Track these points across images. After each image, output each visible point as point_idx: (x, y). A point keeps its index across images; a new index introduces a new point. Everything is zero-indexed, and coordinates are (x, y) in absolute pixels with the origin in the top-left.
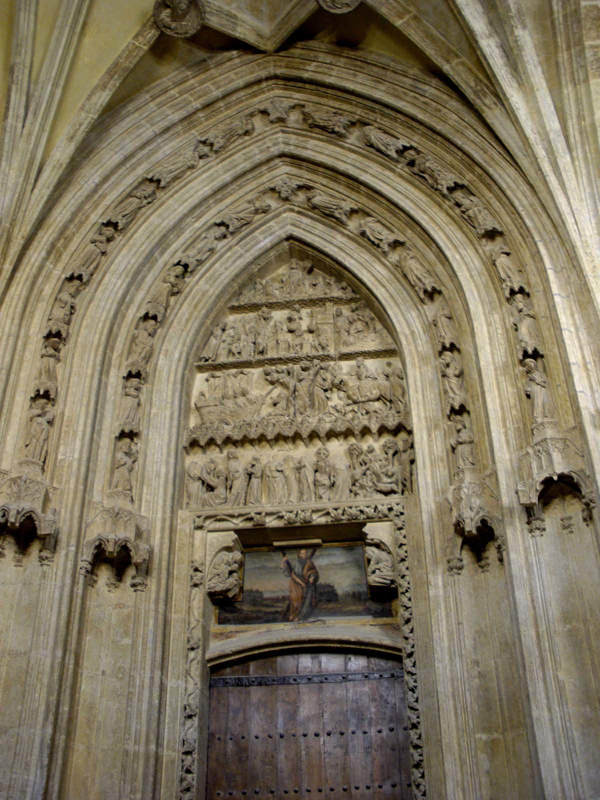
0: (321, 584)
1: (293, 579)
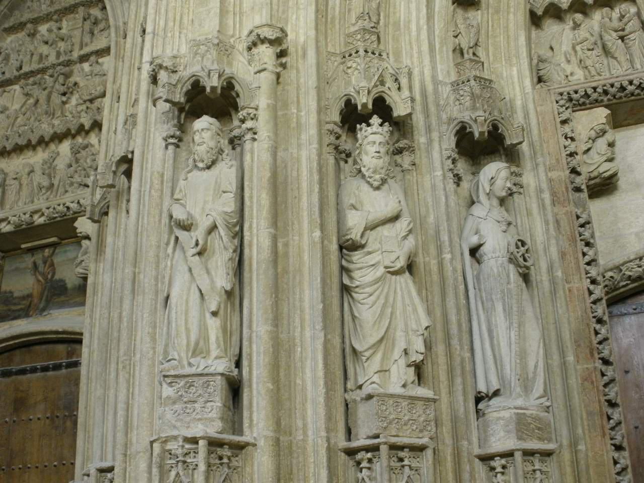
0: (56, 280)
1: (36, 277)
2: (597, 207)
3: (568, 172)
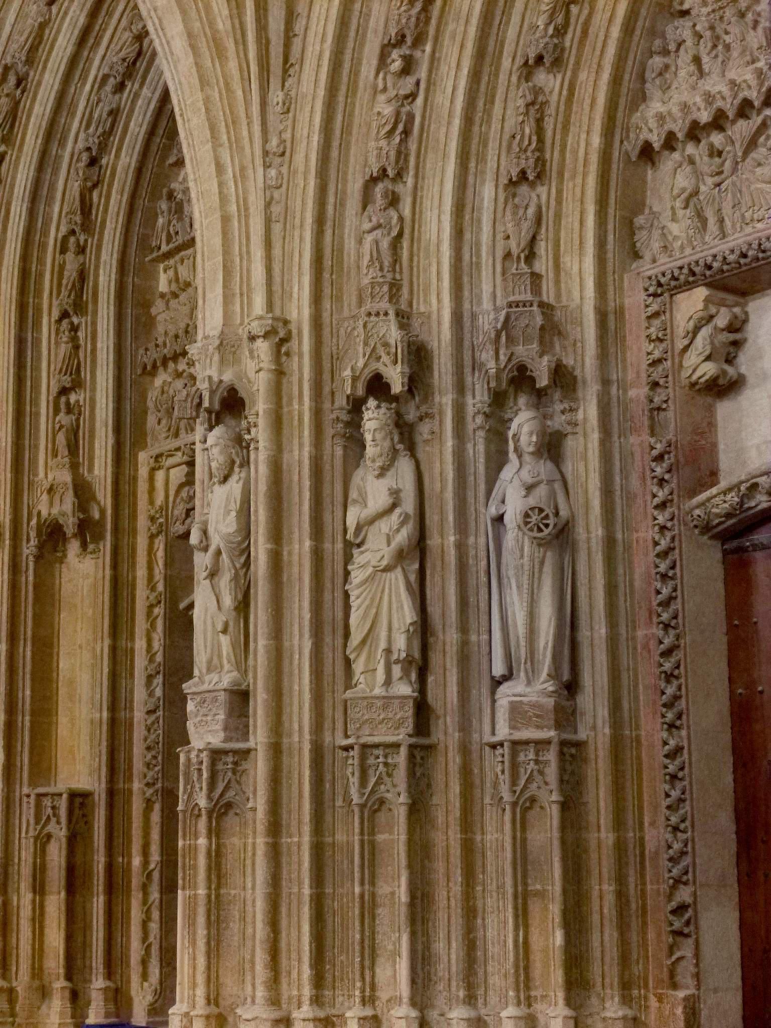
2: (724, 409)
3: (646, 389)
